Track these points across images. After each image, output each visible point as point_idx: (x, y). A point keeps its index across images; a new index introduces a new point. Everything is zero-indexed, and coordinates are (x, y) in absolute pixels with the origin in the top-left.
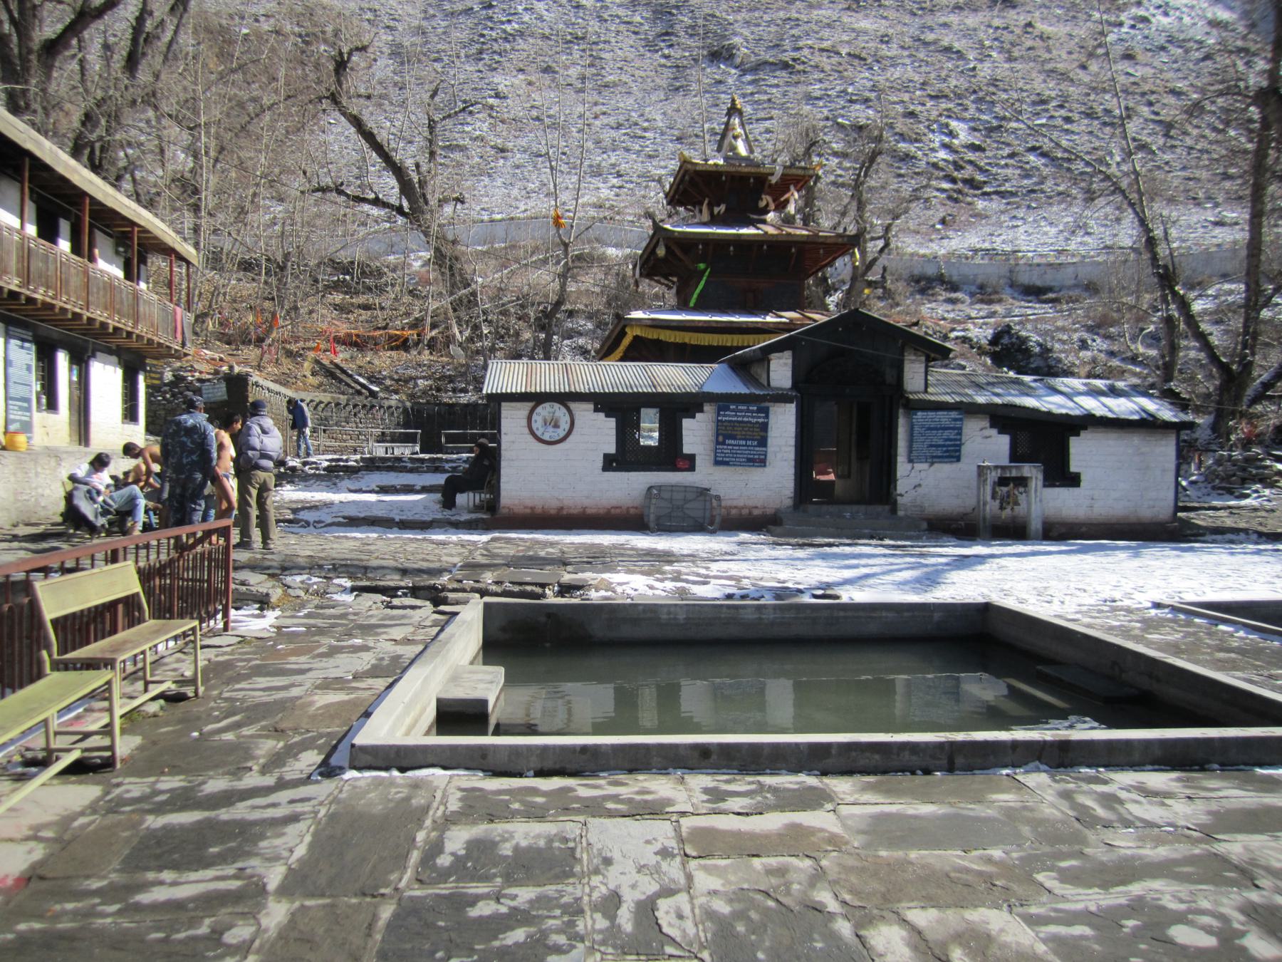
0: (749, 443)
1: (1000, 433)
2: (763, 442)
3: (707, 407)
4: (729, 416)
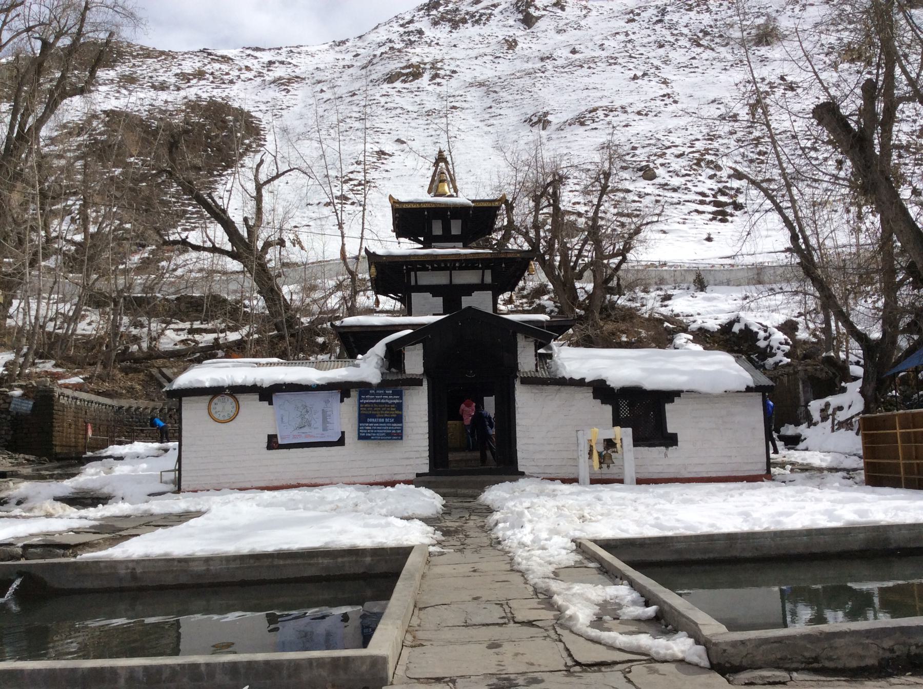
0: (387, 420)
2: (399, 419)
4: (369, 399)
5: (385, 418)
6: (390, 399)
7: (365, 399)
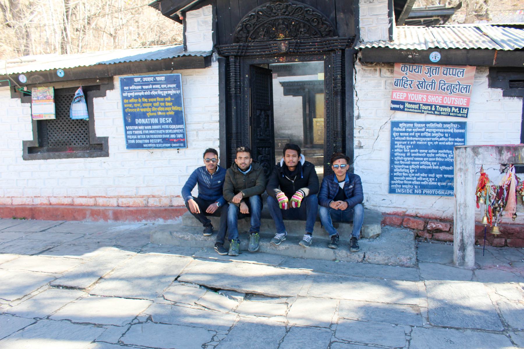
0: (162, 120)
1: (505, 95)
2: (178, 118)
3: (117, 81)
4: (135, 91)
5: (158, 117)
6: (163, 90)
7: (130, 91)
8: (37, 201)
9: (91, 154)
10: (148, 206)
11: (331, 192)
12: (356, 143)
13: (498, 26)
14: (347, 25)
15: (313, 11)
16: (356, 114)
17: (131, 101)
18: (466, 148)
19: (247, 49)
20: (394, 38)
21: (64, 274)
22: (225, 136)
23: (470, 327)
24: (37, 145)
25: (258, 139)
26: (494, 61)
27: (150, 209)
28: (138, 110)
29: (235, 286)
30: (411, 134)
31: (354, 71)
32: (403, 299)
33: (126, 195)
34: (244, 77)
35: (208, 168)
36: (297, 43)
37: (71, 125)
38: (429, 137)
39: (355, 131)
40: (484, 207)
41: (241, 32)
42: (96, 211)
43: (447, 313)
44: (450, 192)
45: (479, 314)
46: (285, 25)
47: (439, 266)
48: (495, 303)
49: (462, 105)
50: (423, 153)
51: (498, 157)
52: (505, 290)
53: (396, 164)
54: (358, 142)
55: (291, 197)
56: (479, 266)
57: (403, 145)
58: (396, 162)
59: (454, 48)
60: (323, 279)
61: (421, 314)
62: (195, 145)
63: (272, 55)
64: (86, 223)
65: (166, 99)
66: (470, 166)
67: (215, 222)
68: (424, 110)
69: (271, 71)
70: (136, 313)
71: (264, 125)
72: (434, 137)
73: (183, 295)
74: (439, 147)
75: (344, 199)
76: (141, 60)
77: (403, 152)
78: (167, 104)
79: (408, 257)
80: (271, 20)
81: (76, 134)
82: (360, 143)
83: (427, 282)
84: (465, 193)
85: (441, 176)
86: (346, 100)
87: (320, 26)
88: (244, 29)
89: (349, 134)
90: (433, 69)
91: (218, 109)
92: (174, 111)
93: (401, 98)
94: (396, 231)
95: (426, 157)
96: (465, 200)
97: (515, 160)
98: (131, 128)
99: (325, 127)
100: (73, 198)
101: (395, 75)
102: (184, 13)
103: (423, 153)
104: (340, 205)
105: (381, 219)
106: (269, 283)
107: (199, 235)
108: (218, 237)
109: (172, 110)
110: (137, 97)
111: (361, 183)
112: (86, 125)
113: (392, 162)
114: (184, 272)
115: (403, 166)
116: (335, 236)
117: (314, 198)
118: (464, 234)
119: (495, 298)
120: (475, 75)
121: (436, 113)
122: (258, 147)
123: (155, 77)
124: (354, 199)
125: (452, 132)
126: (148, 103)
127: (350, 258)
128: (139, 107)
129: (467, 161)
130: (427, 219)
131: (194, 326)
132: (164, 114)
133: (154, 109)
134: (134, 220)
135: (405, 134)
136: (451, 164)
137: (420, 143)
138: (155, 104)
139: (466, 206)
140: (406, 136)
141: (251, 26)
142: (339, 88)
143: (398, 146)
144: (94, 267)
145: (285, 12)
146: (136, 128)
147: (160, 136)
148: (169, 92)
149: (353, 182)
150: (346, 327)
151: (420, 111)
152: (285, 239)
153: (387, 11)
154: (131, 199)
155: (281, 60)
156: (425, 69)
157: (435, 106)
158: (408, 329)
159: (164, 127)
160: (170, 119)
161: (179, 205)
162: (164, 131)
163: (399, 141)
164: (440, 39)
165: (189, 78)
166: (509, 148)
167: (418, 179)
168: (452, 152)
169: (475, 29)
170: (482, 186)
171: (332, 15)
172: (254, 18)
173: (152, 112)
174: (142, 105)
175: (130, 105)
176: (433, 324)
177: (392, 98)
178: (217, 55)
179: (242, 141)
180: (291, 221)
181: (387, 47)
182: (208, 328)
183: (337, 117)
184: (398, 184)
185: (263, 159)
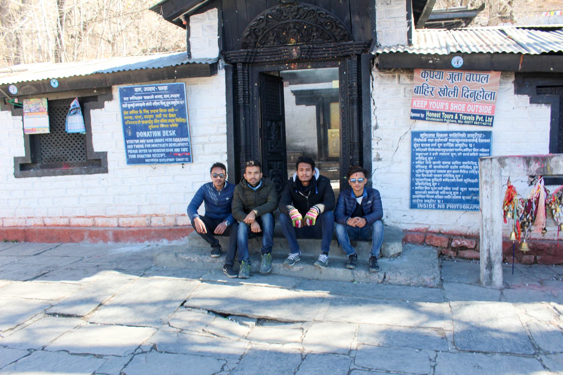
0: (165, 133)
1: (532, 102)
2: (183, 131)
3: (116, 91)
4: (136, 102)
5: (161, 129)
6: (165, 100)
7: (130, 101)
8: (31, 223)
9: (89, 171)
10: (151, 226)
11: (348, 208)
12: (374, 155)
13: (524, 28)
14: (363, 28)
15: (326, 14)
16: (373, 124)
17: (131, 112)
18: (491, 159)
19: (256, 56)
20: (413, 42)
21: (61, 301)
22: (233, 149)
23: (499, 351)
24: (30, 162)
25: (269, 152)
26: (520, 66)
27: (153, 229)
28: (139, 122)
29: (246, 311)
30: (432, 145)
31: (371, 77)
32: (427, 322)
33: (126, 214)
34: (253, 85)
35: (216, 184)
36: (309, 48)
37: (67, 139)
38: (452, 148)
39: (372, 142)
40: (512, 222)
41: (249, 37)
42: (95, 232)
43: (474, 336)
44: (475, 206)
45: (508, 337)
46: (296, 29)
47: (465, 286)
48: (525, 325)
49: (487, 113)
50: (446, 165)
51: (526, 169)
52: (535, 310)
53: (418, 178)
54: (376, 154)
55: (305, 215)
56: (507, 285)
57: (425, 156)
58: (417, 175)
59: (477, 52)
60: (341, 302)
61: (446, 338)
62: (201, 159)
63: (282, 62)
64: (84, 245)
65: (170, 110)
66: (496, 178)
67: (224, 243)
68: (447, 119)
69: (282, 78)
70: (139, 342)
71: (275, 137)
72: (458, 148)
73: (190, 322)
74: (462, 159)
75: (362, 215)
76: (141, 69)
77: (425, 164)
78: (170, 115)
79: (432, 277)
80: (282, 24)
81: (72, 149)
82: (378, 155)
83: (452, 304)
84: (492, 207)
85: (466, 189)
86: (363, 109)
87: (334, 30)
88: (253, 34)
89: (367, 146)
90: (455, 75)
91: (225, 121)
92: (177, 123)
93: (422, 106)
94: (418, 249)
95: (449, 169)
96: (492, 215)
97: (544, 171)
98: (131, 141)
99: (340, 138)
100: (69, 219)
101: (415, 81)
102: (187, 18)
103: (446, 165)
104: (358, 222)
105: (402, 237)
106: (283, 307)
107: (207, 257)
108: (227, 258)
109: (175, 122)
110: (137, 108)
111: (380, 198)
112: (83, 139)
113: (413, 175)
114: (191, 297)
115: (424, 179)
116: (353, 256)
117: (330, 215)
118: (491, 251)
119: (525, 319)
120: (500, 81)
121: (459, 121)
122: (268, 161)
123: (156, 87)
124: (372, 216)
125: (476, 141)
126: (150, 114)
127: (370, 279)
128: (141, 120)
129: (493, 173)
130: (451, 236)
131: (202, 355)
132: (167, 126)
133: (156, 121)
134: (136, 241)
135: (426, 145)
136: (476, 176)
137: (443, 154)
138: (157, 116)
139: (492, 221)
140: (428, 147)
141: (259, 31)
142: (355, 96)
143: (419, 158)
144: (93, 292)
145: (296, 15)
146: (137, 141)
147: (164, 150)
148: (173, 103)
149: (372, 197)
150: (365, 353)
151: (442, 120)
152: (299, 260)
153: (405, 13)
154: (132, 219)
155: (293, 67)
156: (447, 75)
157: (458, 114)
158: (432, 355)
159: (167, 140)
160: (174, 132)
161: (185, 224)
162: (167, 145)
163: (420, 152)
164: (462, 43)
165: (193, 87)
166: (537, 159)
167: (441, 193)
168: (477, 164)
169: (499, 31)
170: (509, 199)
171: (347, 18)
172: (263, 22)
173: (154, 124)
174: (143, 116)
175: (131, 117)
176: (459, 348)
177: (412, 106)
178: (223, 62)
179: (252, 154)
180: (305, 240)
181: (406, 52)
182: (218, 357)
183: (353, 128)
184: (420, 199)
185: (274, 173)
